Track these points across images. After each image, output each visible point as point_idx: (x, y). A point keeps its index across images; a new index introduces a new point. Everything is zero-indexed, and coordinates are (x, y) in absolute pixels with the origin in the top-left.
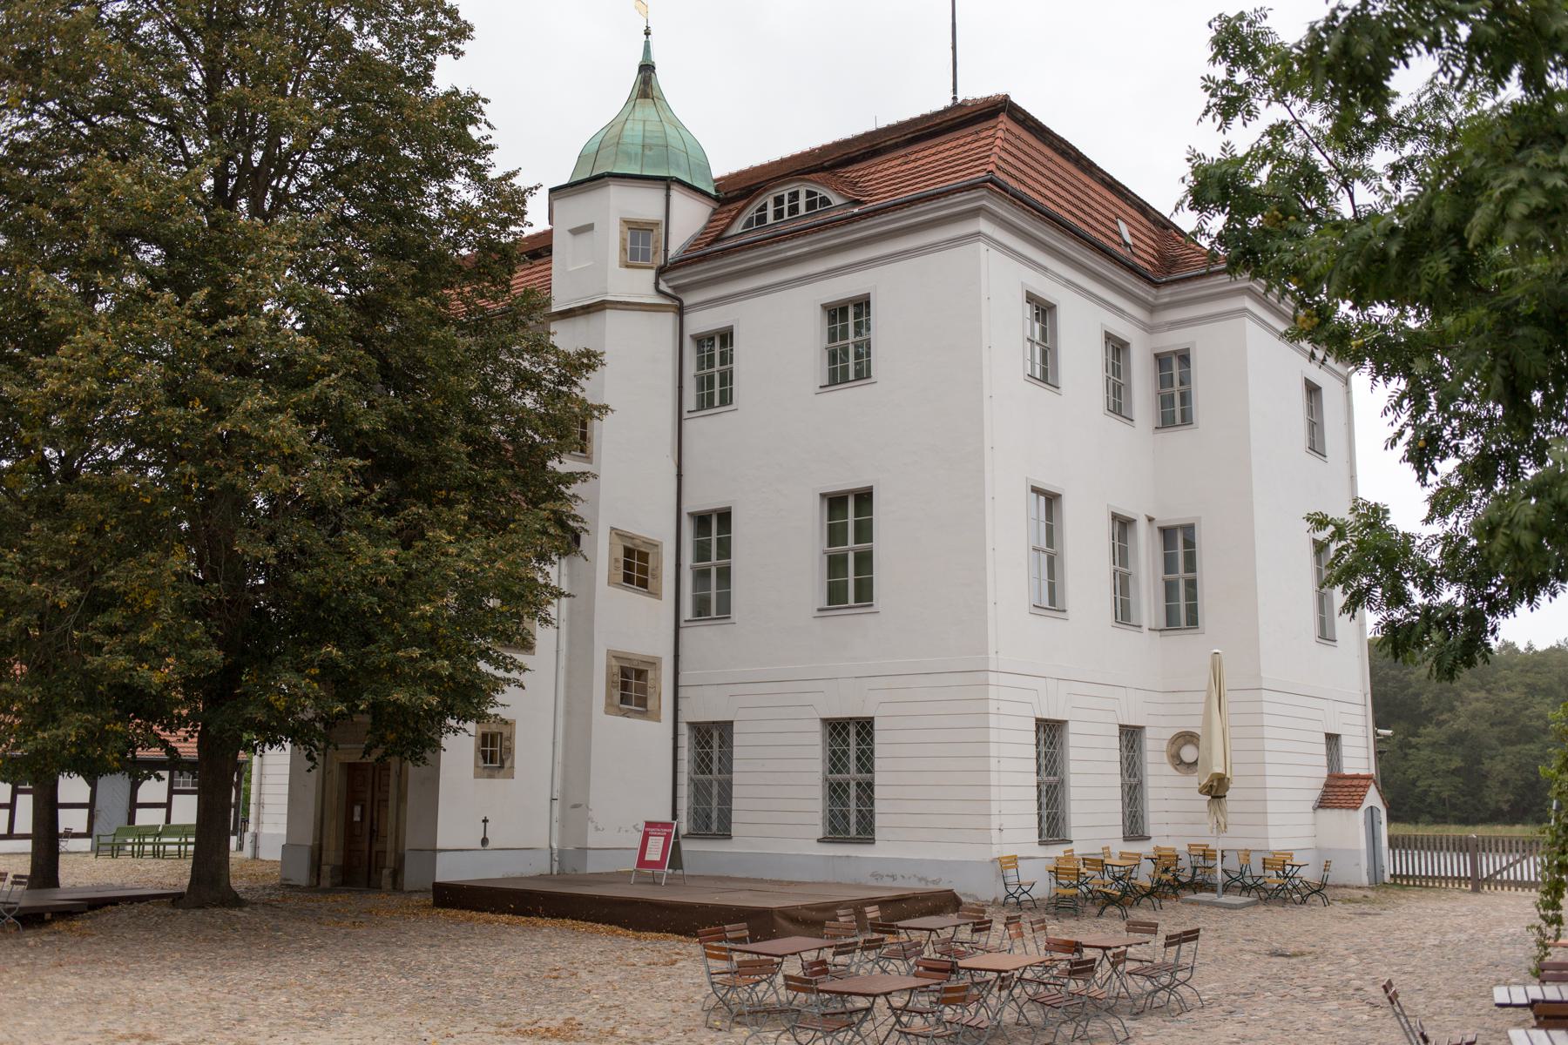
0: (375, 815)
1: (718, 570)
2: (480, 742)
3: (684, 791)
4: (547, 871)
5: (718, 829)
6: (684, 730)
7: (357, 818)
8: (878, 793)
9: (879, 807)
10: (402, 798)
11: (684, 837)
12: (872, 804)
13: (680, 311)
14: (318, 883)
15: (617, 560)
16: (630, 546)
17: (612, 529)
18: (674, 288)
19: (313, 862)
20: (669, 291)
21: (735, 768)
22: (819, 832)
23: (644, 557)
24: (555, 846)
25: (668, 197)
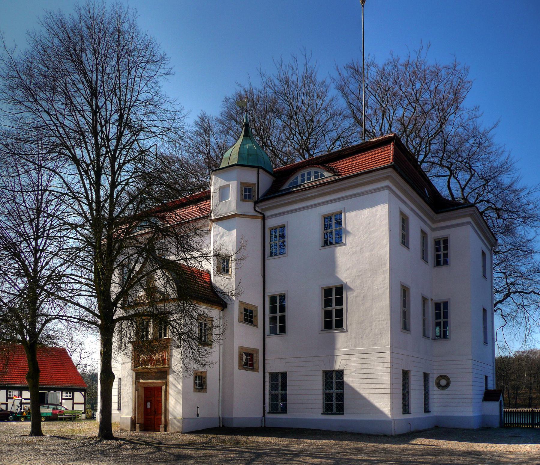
5: (281, 411)
6: (267, 375)
7: (149, 407)
8: (345, 397)
9: (345, 402)
12: (343, 401)
13: (264, 219)
15: (241, 313)
16: (246, 308)
17: (240, 301)
18: (262, 209)
20: (259, 211)
22: (321, 411)
23: (251, 312)
24: (221, 417)
25: (258, 174)
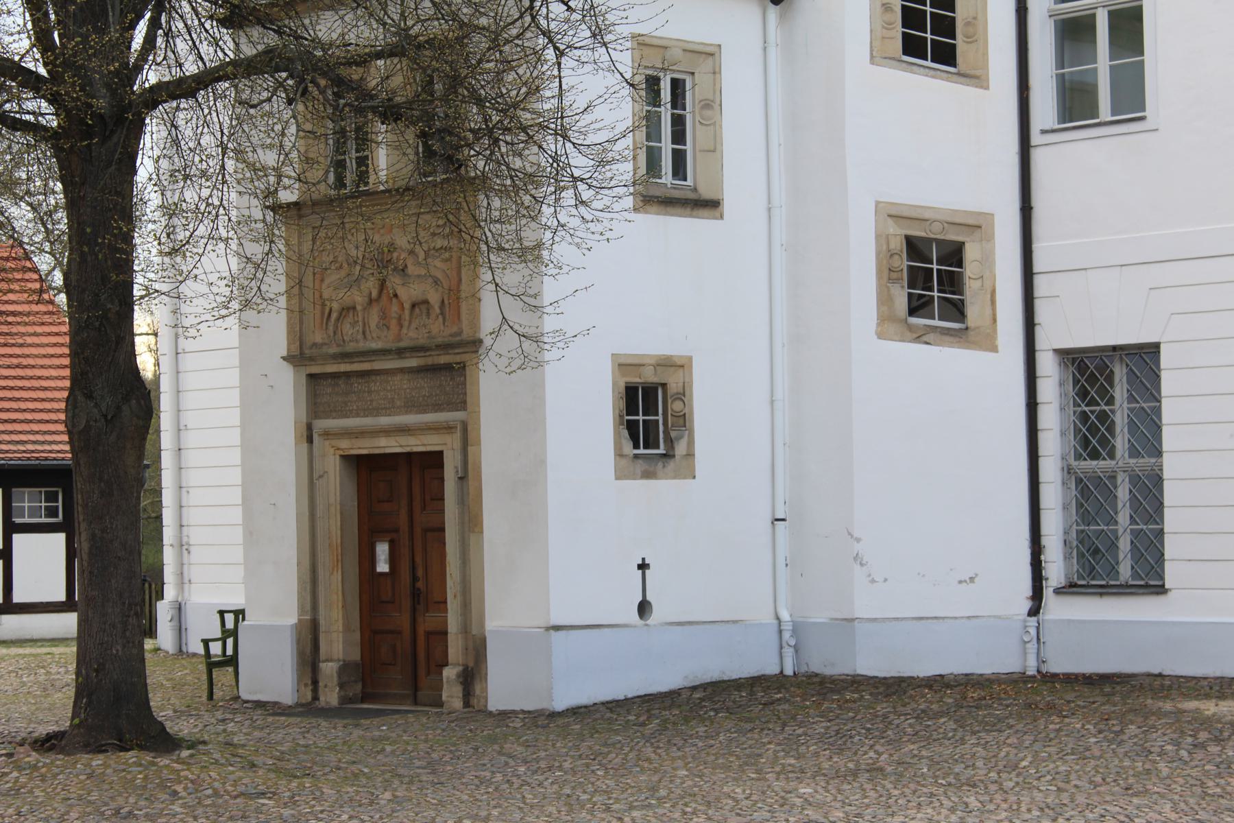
0: (419, 560)
1: (1111, 14)
2: (622, 404)
3: (1052, 495)
4: (773, 669)
5: (1135, 575)
6: (1047, 365)
7: (383, 567)
10: (472, 521)
11: (1058, 591)
14: (316, 698)
19: (301, 654)
21: (1166, 446)
24: (785, 615)
